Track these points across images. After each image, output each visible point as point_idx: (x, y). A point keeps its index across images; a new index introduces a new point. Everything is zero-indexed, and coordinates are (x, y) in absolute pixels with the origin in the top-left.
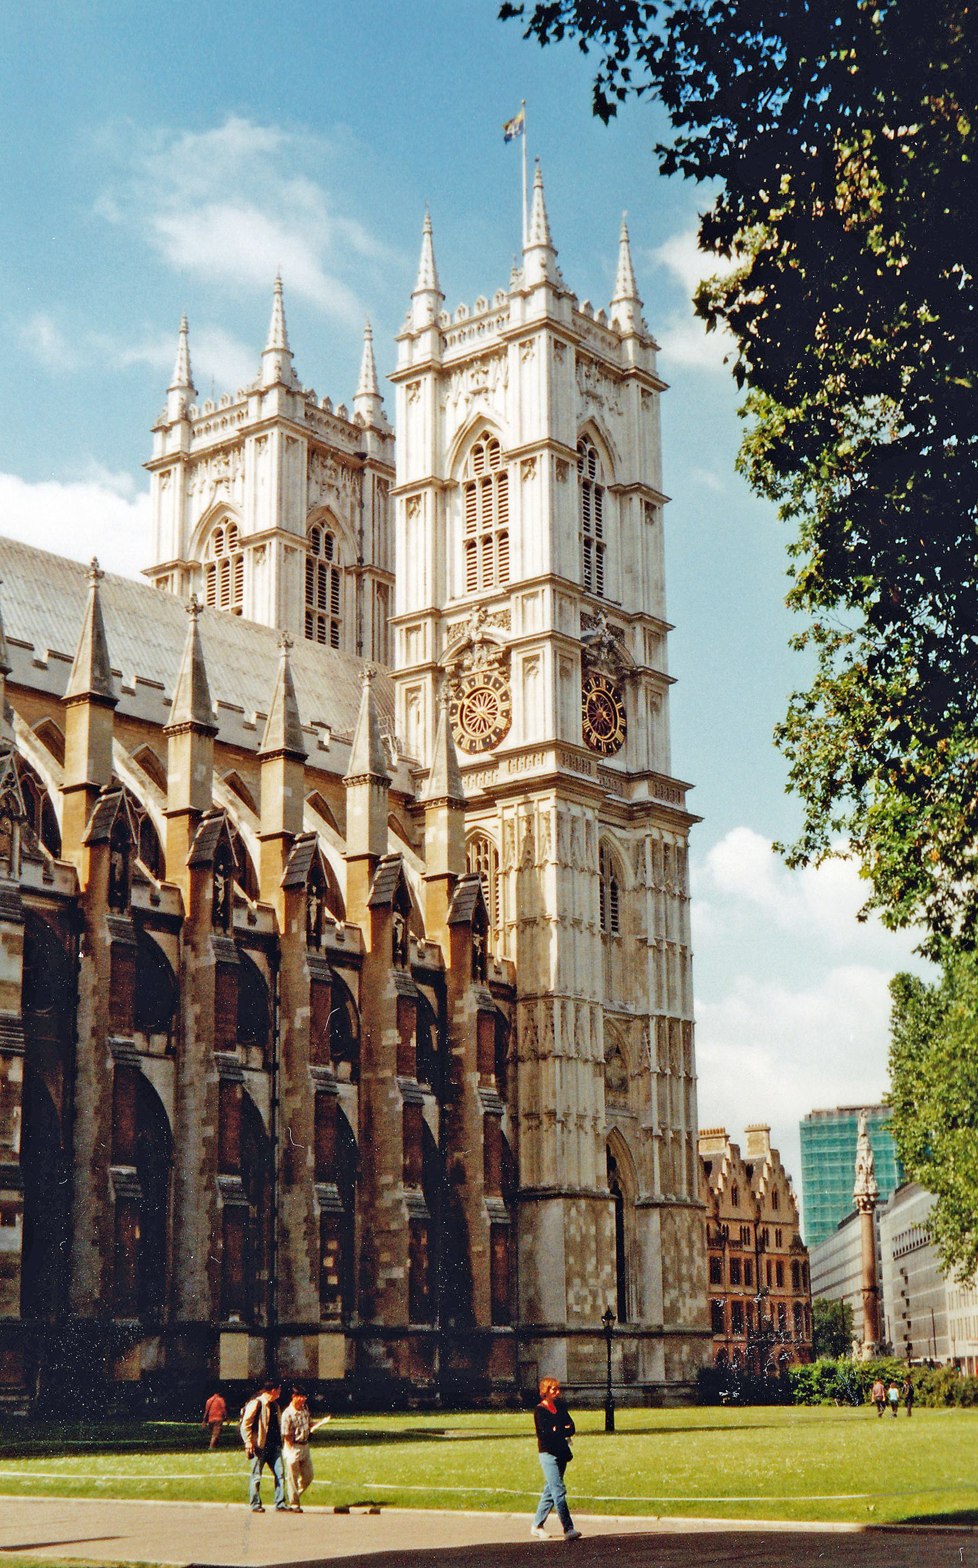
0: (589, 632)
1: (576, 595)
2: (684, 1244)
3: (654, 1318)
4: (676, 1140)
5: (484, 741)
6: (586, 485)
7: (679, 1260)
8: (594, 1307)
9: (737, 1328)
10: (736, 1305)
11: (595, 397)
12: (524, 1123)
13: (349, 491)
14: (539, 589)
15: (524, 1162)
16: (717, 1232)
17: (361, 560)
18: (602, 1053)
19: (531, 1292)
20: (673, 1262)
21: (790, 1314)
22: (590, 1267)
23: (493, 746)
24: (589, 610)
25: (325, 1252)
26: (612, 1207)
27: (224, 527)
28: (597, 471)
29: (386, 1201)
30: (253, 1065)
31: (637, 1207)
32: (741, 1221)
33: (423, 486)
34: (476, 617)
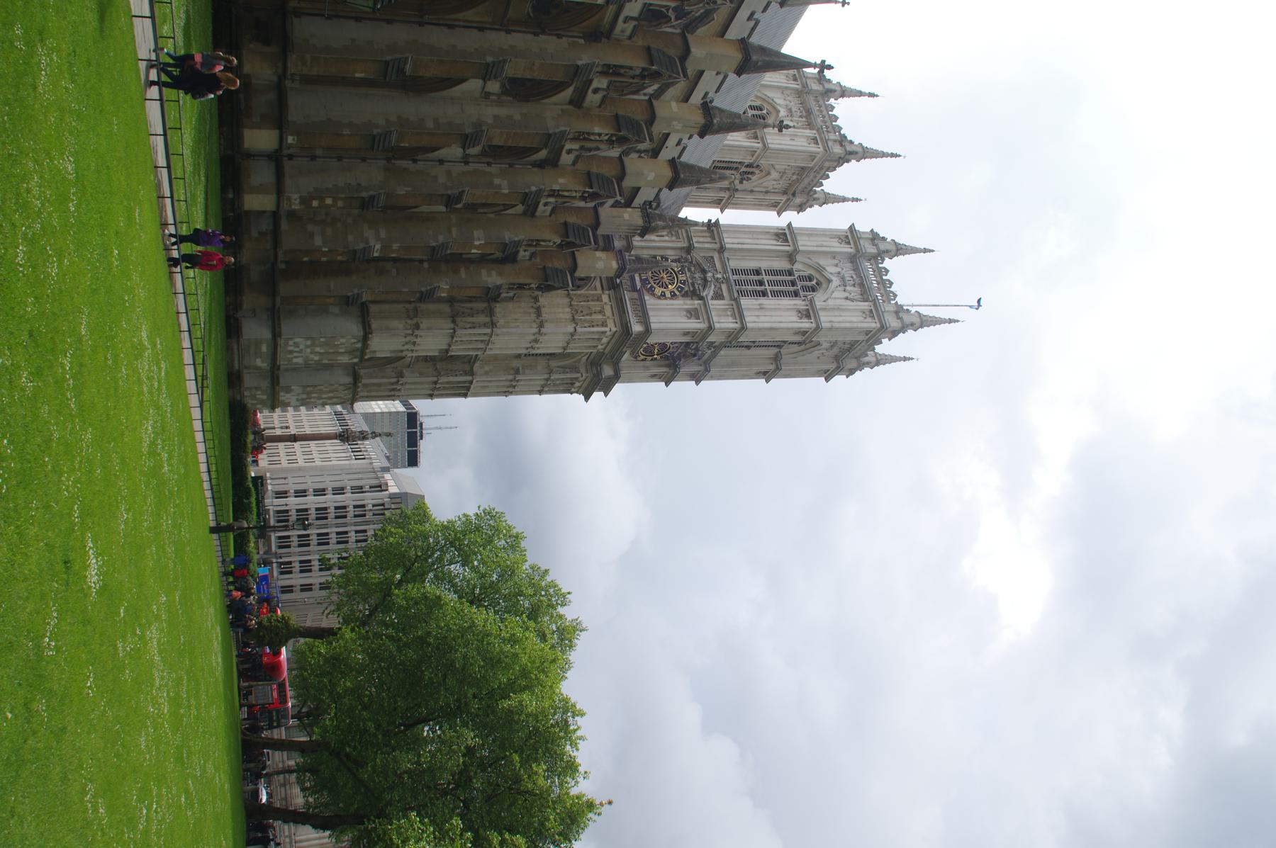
2: (331, 395)
4: (393, 390)
5: (647, 279)
8: (291, 352)
11: (832, 347)
13: (776, 186)
14: (738, 321)
18: (453, 354)
20: (320, 390)
22: (318, 349)
25: (335, 199)
27: (765, 112)
29: (369, 233)
31: (354, 368)
33: (794, 244)
34: (719, 276)
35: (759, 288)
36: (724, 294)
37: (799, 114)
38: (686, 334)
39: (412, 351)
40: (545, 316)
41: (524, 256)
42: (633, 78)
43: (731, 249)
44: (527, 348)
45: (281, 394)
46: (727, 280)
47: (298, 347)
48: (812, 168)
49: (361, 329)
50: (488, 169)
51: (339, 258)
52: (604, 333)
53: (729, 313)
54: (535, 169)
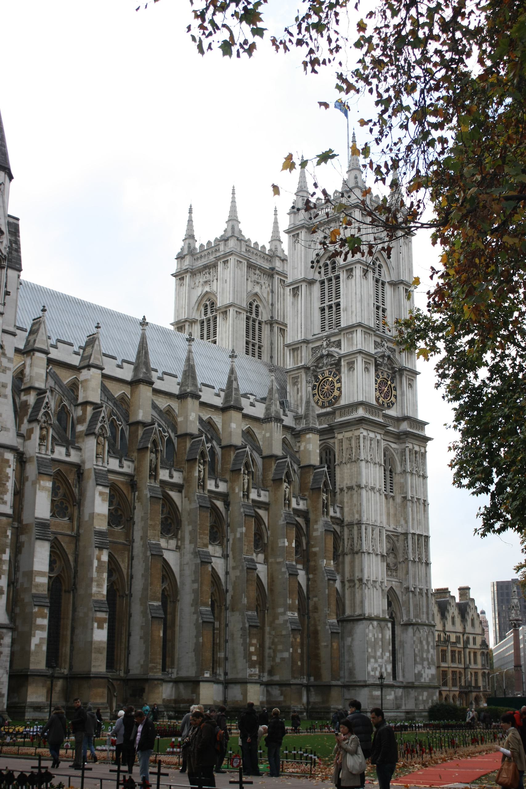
0: (379, 350)
1: (372, 333)
2: (424, 643)
3: (410, 678)
4: (421, 593)
5: (328, 402)
6: (377, 281)
7: (422, 650)
9: (454, 685)
10: (454, 673)
12: (347, 583)
14: (355, 329)
15: (347, 603)
16: (444, 638)
17: (272, 317)
18: (385, 551)
19: (351, 665)
20: (419, 651)
21: (480, 678)
22: (379, 654)
23: (334, 404)
24: (378, 340)
25: (251, 645)
26: (390, 625)
27: (208, 303)
28: (382, 274)
29: (281, 619)
30: (217, 555)
32: (456, 632)
33: (300, 282)
34: (325, 343)
35: (334, 309)
36: (337, 339)
37: (207, 275)
38: (367, 369)
39: (382, 582)
40: (354, 484)
41: (304, 504)
42: (157, 459)
43: (306, 333)
44: (381, 494)
45: (423, 680)
46: (328, 337)
47: (376, 668)
48: (248, 260)
49: (361, 622)
50: (231, 541)
51: (298, 640)
52: (364, 438)
53: (350, 336)
54: (230, 508)
